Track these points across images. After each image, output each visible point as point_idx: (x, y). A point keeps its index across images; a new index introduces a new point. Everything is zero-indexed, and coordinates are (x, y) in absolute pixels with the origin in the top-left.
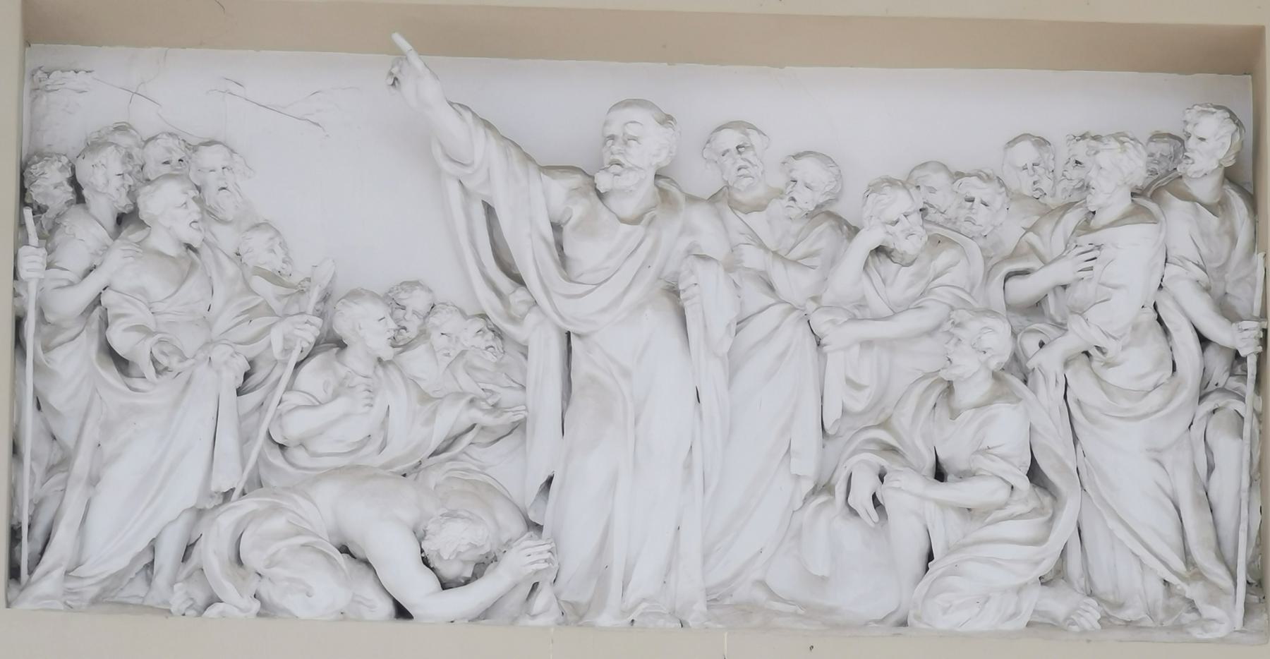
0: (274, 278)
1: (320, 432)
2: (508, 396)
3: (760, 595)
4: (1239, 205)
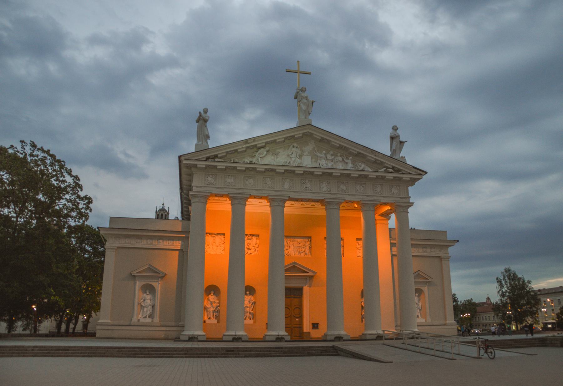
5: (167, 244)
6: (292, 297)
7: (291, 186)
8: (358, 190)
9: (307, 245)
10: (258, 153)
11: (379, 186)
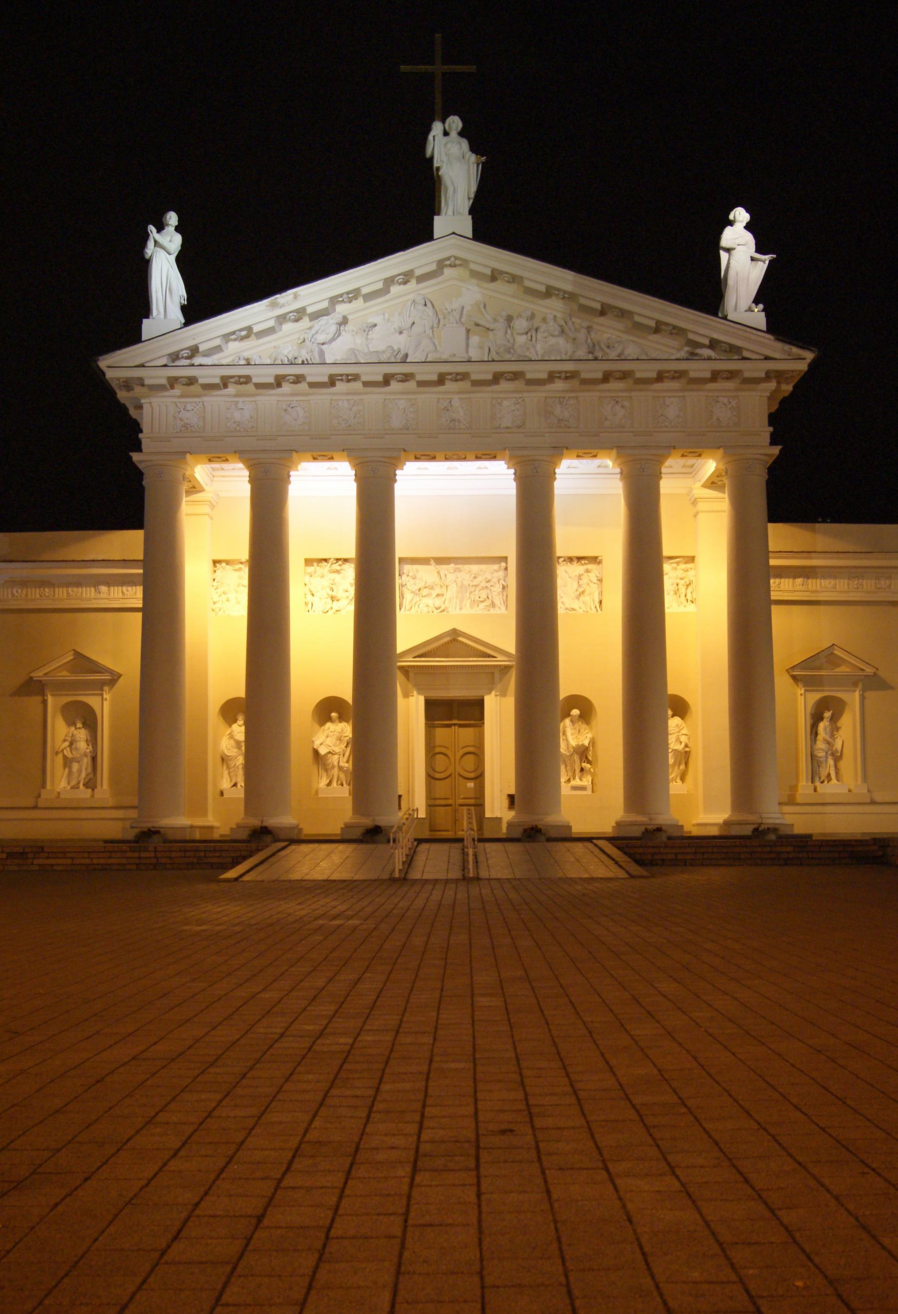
5: (120, 595)
6: (455, 725)
8: (606, 419)
9: (495, 580)
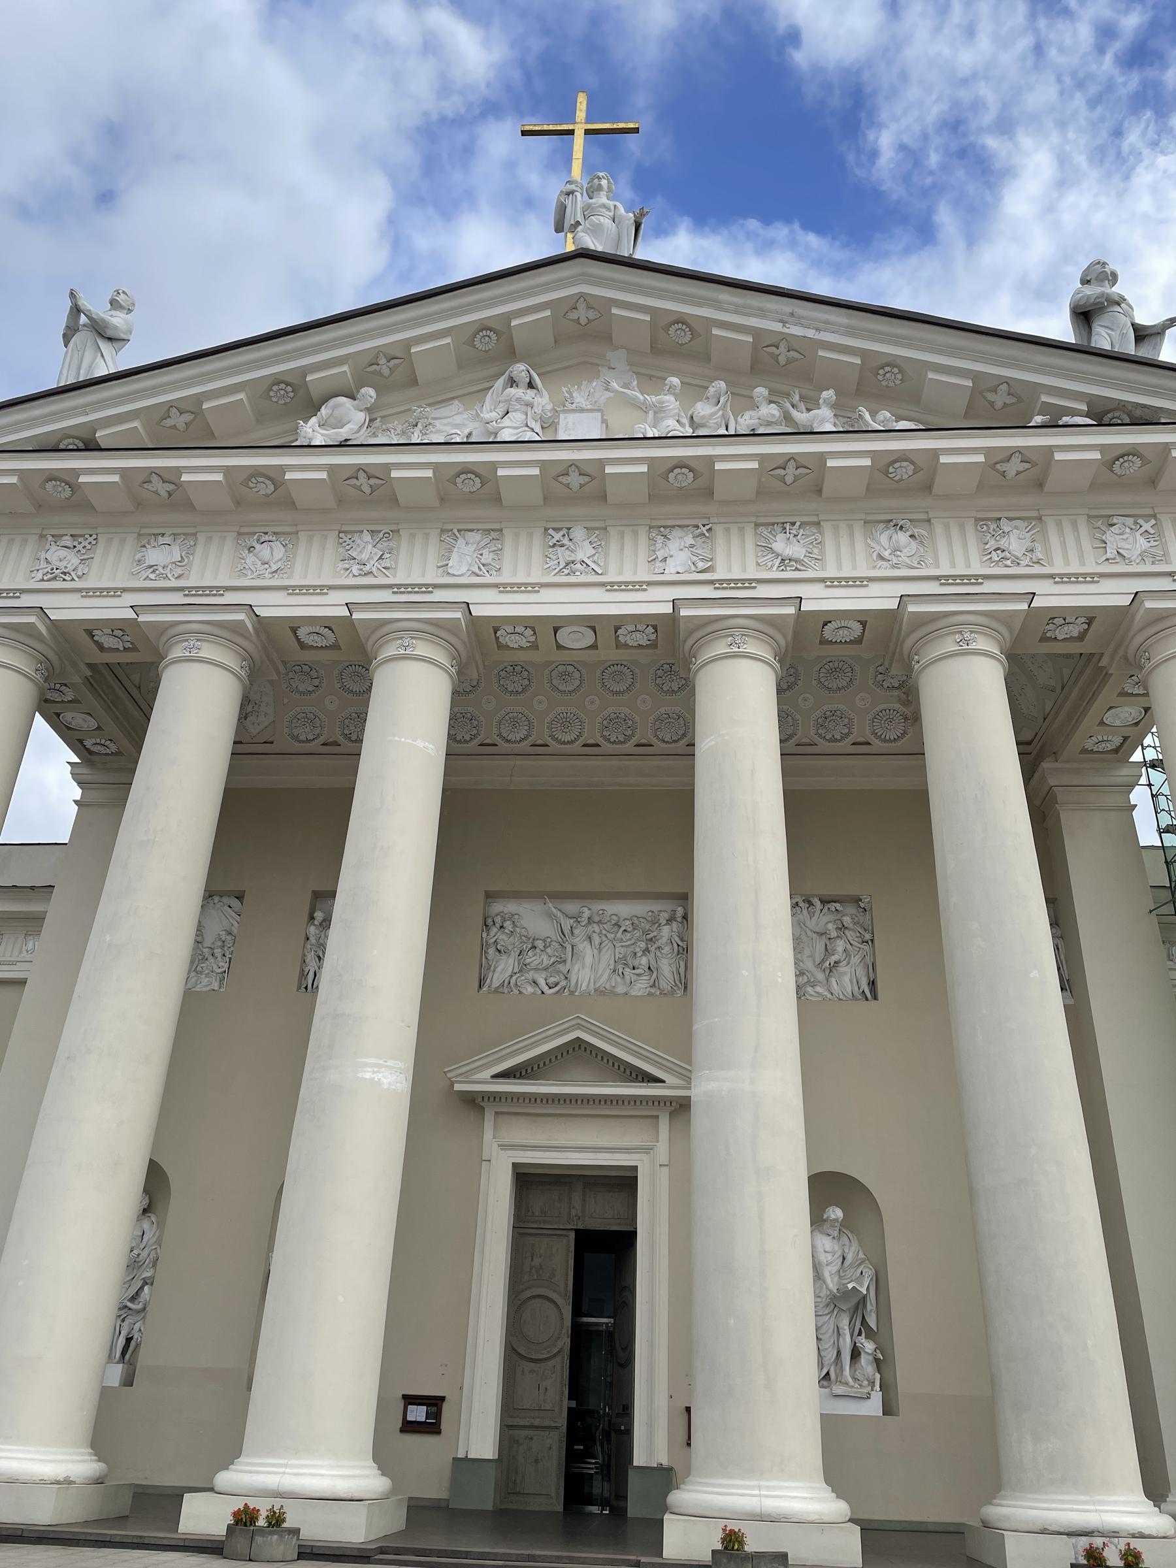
0: (526, 937)
1: (531, 962)
2: (563, 956)
3: (604, 989)
4: (685, 922)
7: (489, 561)
10: (314, 420)
11: (1017, 528)
